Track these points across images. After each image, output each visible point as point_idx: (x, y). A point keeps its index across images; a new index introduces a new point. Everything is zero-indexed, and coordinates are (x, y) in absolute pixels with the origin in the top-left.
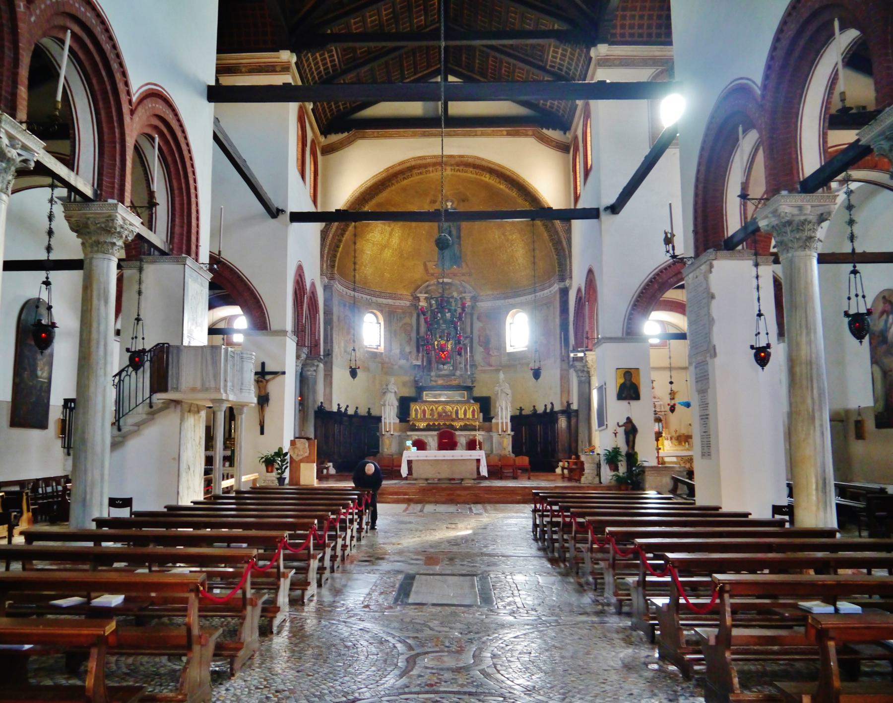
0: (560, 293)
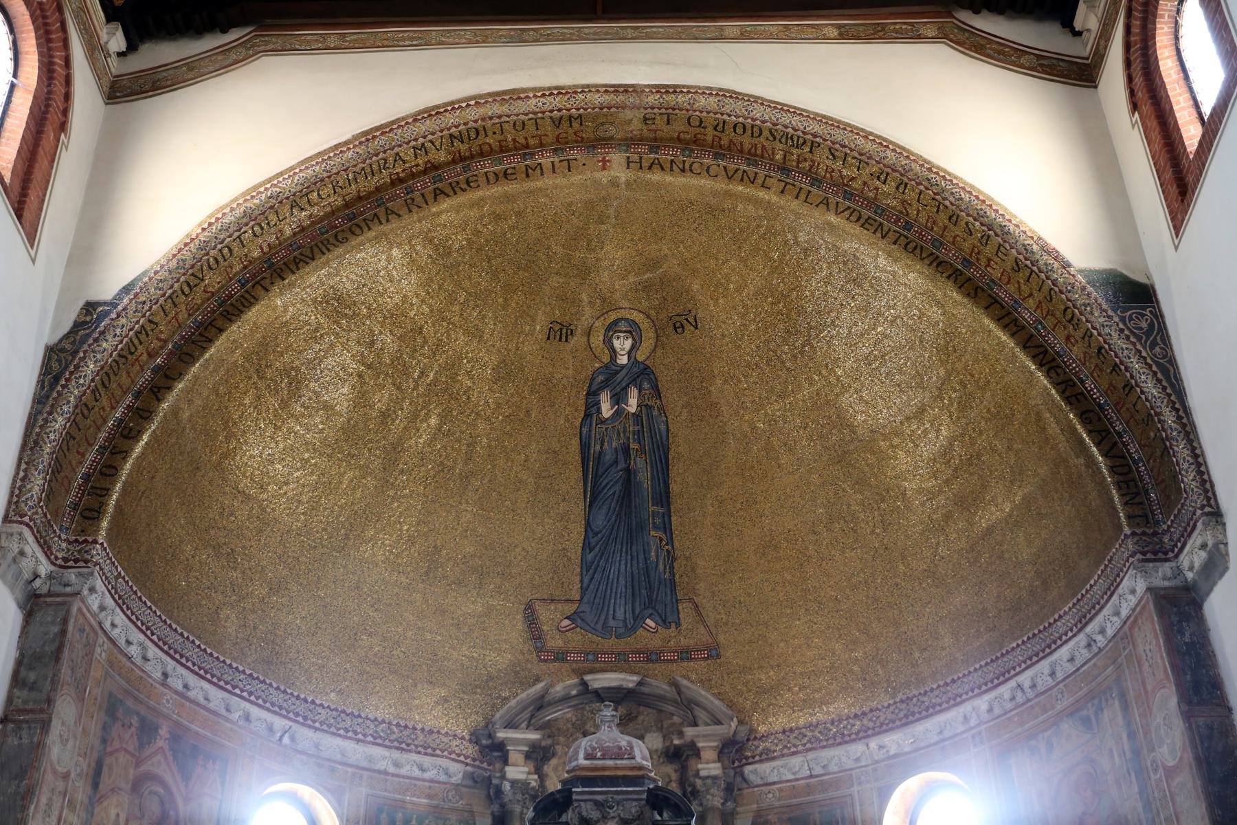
0: (1161, 612)
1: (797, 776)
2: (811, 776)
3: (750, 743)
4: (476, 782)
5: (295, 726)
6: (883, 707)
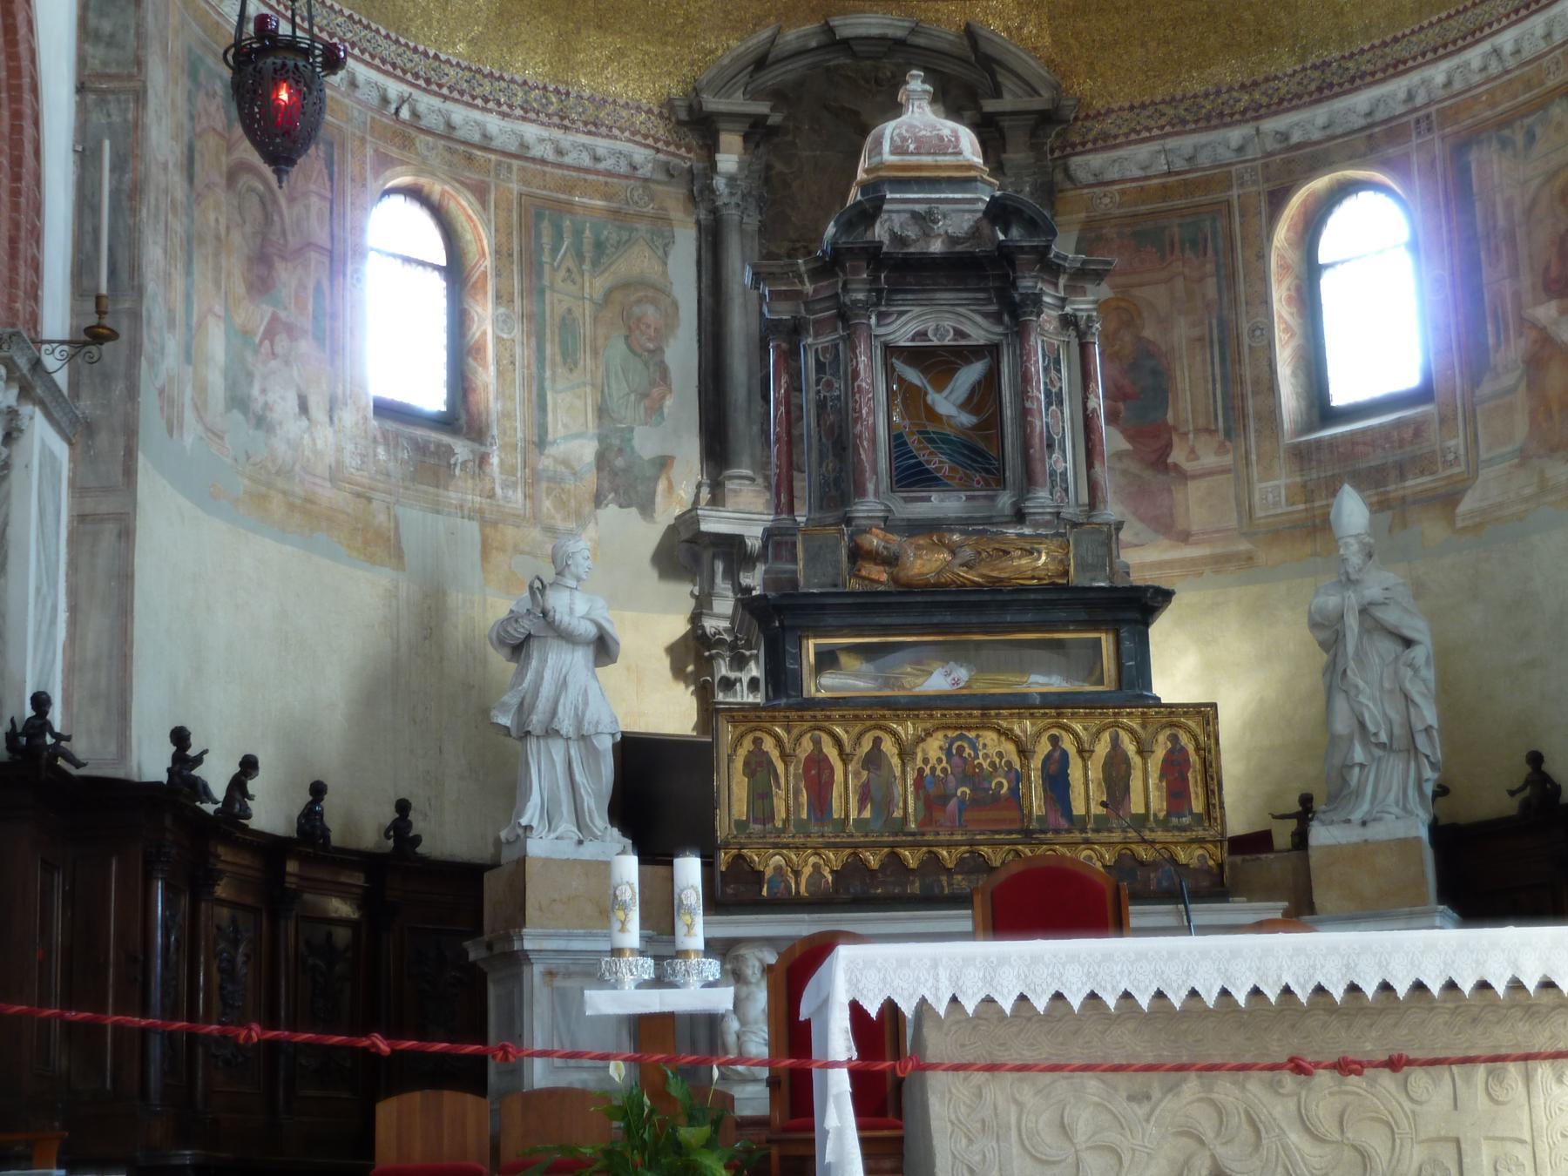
1: (1150, 172)
2: (1169, 173)
3: (1080, 123)
4: (672, 176)
5: (416, 94)
6: (1285, 75)
